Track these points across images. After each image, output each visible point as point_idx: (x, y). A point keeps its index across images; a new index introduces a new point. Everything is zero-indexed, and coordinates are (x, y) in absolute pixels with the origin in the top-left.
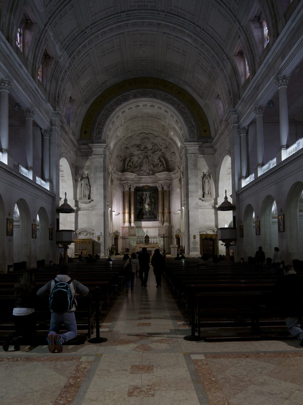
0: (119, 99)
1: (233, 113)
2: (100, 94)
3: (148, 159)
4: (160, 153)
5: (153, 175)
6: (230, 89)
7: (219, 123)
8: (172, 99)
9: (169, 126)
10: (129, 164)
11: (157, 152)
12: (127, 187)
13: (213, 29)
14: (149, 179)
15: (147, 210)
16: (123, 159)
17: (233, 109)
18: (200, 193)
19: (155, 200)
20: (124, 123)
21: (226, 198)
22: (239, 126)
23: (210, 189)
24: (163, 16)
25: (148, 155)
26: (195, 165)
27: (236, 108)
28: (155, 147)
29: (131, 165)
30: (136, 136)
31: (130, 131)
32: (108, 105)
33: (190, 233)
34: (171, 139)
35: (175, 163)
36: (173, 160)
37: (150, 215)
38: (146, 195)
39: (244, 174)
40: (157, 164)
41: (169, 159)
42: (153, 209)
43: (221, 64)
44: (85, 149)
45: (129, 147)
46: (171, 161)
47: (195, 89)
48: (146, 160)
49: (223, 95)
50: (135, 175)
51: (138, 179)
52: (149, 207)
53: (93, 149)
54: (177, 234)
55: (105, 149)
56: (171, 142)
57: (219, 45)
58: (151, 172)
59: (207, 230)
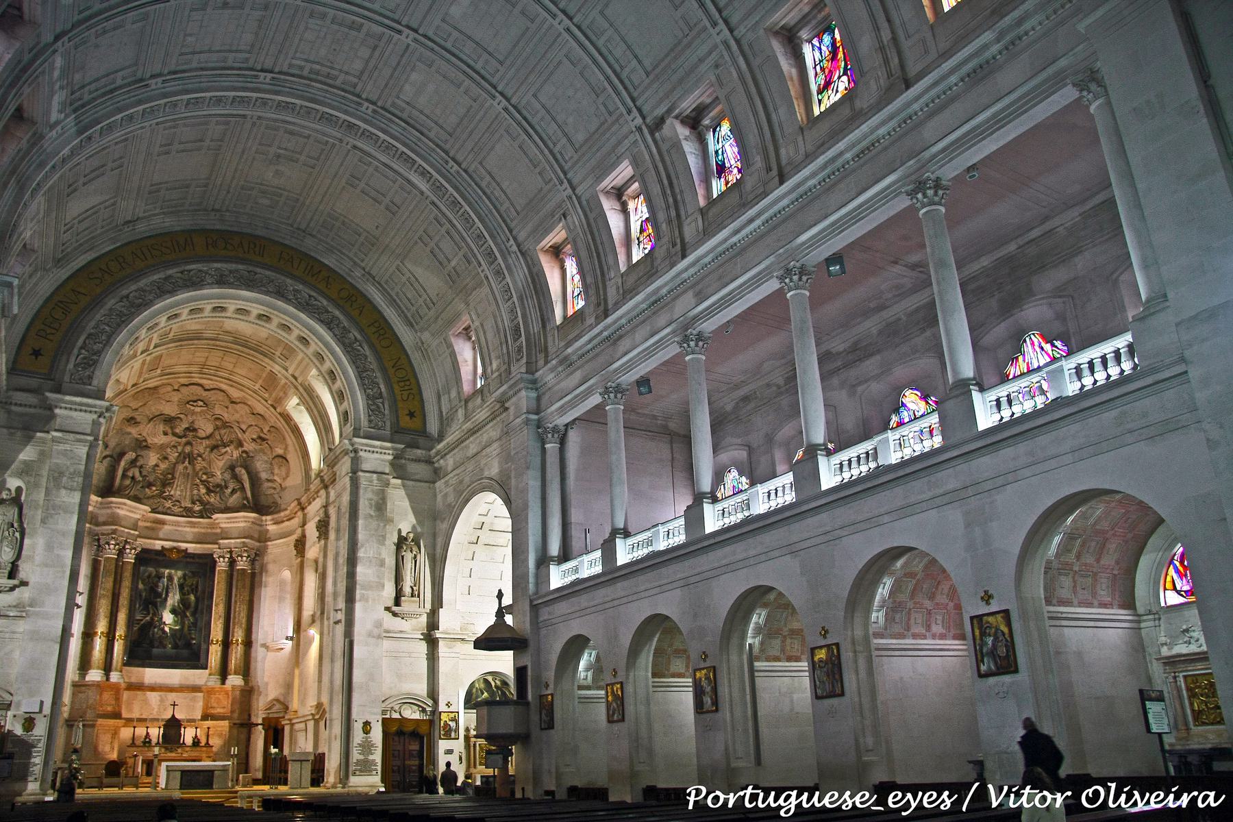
0: (170, 276)
1: (530, 386)
2: (107, 249)
3: (194, 465)
4: (236, 454)
5: (203, 517)
6: (519, 323)
7: (460, 401)
8: (327, 312)
9: (294, 381)
10: (130, 474)
11: (228, 449)
12: (112, 546)
13: (493, 178)
14: (188, 529)
15: (167, 629)
16: (107, 453)
17: (530, 377)
18: (389, 591)
20: (155, 347)
21: (500, 613)
22: (539, 420)
23: (416, 582)
24: (369, 112)
25: (196, 452)
26: (380, 506)
27: (538, 374)
28: (223, 432)
29: (137, 474)
30: (169, 388)
31: (159, 371)
32: (133, 287)
33: (354, 716)
34: (287, 418)
35: (283, 489)
36: (276, 478)
37: (175, 646)
38: (170, 578)
39: (554, 549)
40: (218, 486)
41: (264, 476)
42: (189, 627)
43: (500, 260)
44: (26, 405)
45: (139, 419)
46: (268, 481)
47: (395, 301)
48: (186, 468)
49: (485, 333)
50: (145, 511)
51: (148, 524)
52: (175, 621)
53: (57, 411)
54: (271, 716)
55: (100, 416)
56: (281, 424)
57: (501, 216)
58: (197, 508)
59: (405, 706)
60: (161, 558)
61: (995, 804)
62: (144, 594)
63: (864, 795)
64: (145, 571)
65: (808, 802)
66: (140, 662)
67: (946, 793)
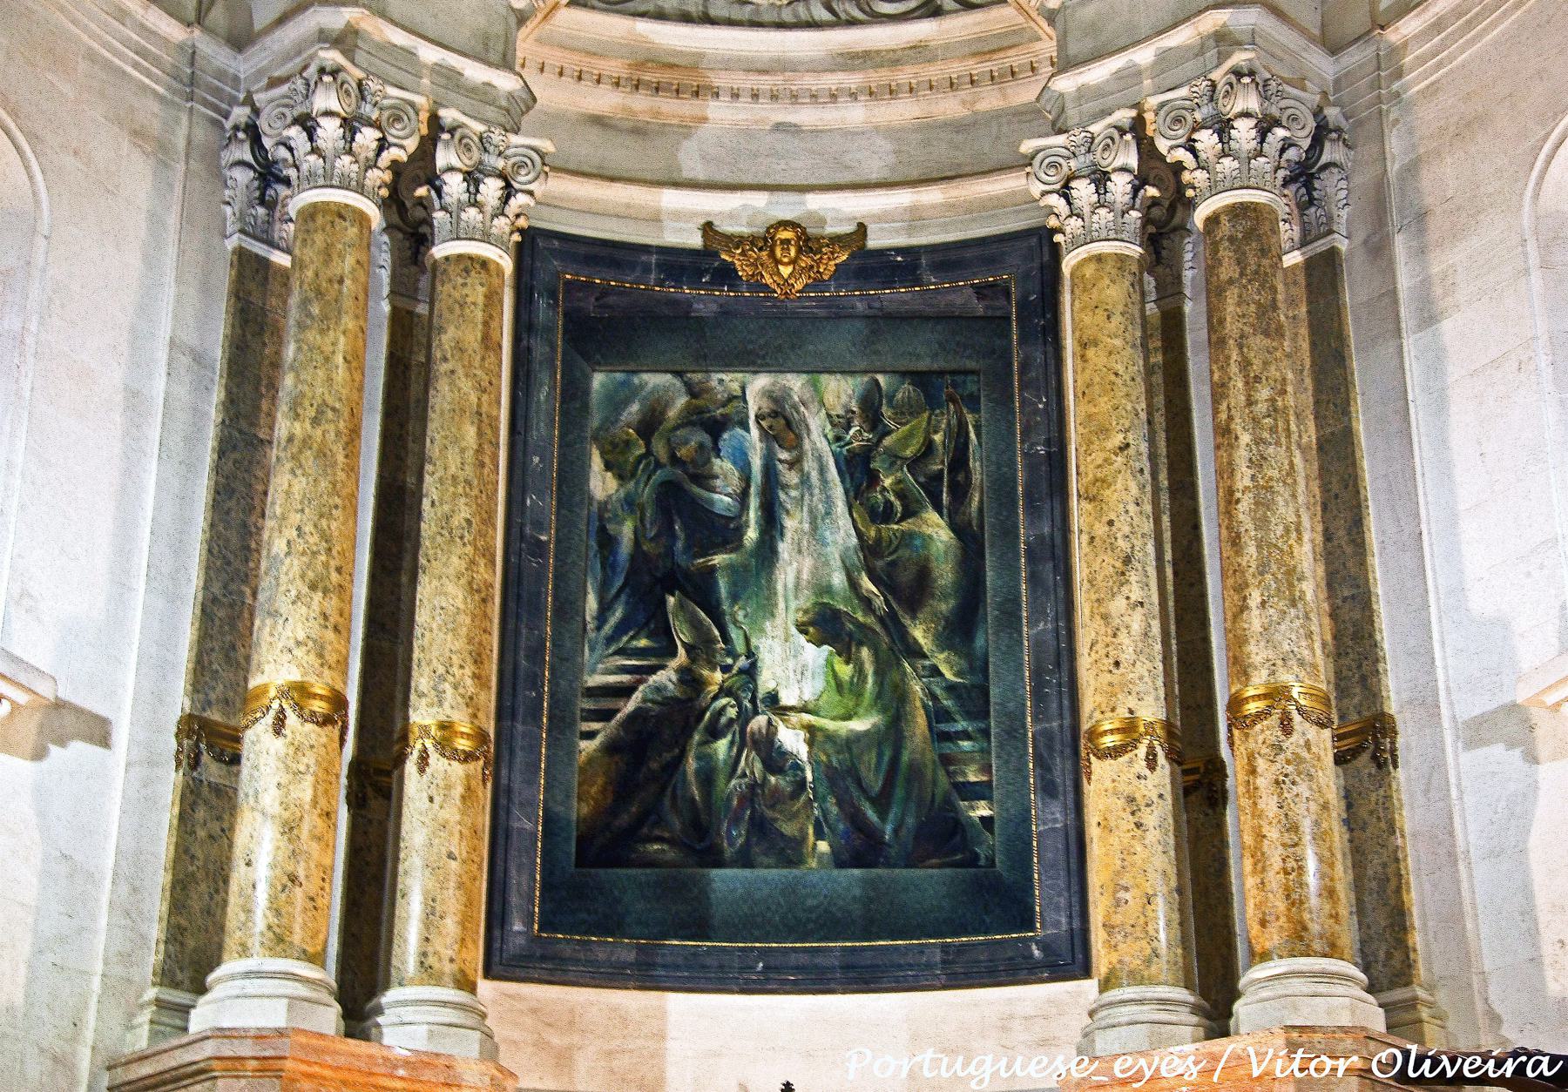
12: (330, 131)
14: (855, 114)
15: (791, 739)
19: (968, 538)
42: (938, 715)
51: (605, 101)
60: (703, 299)
62: (627, 531)
64: (616, 401)
66: (625, 950)
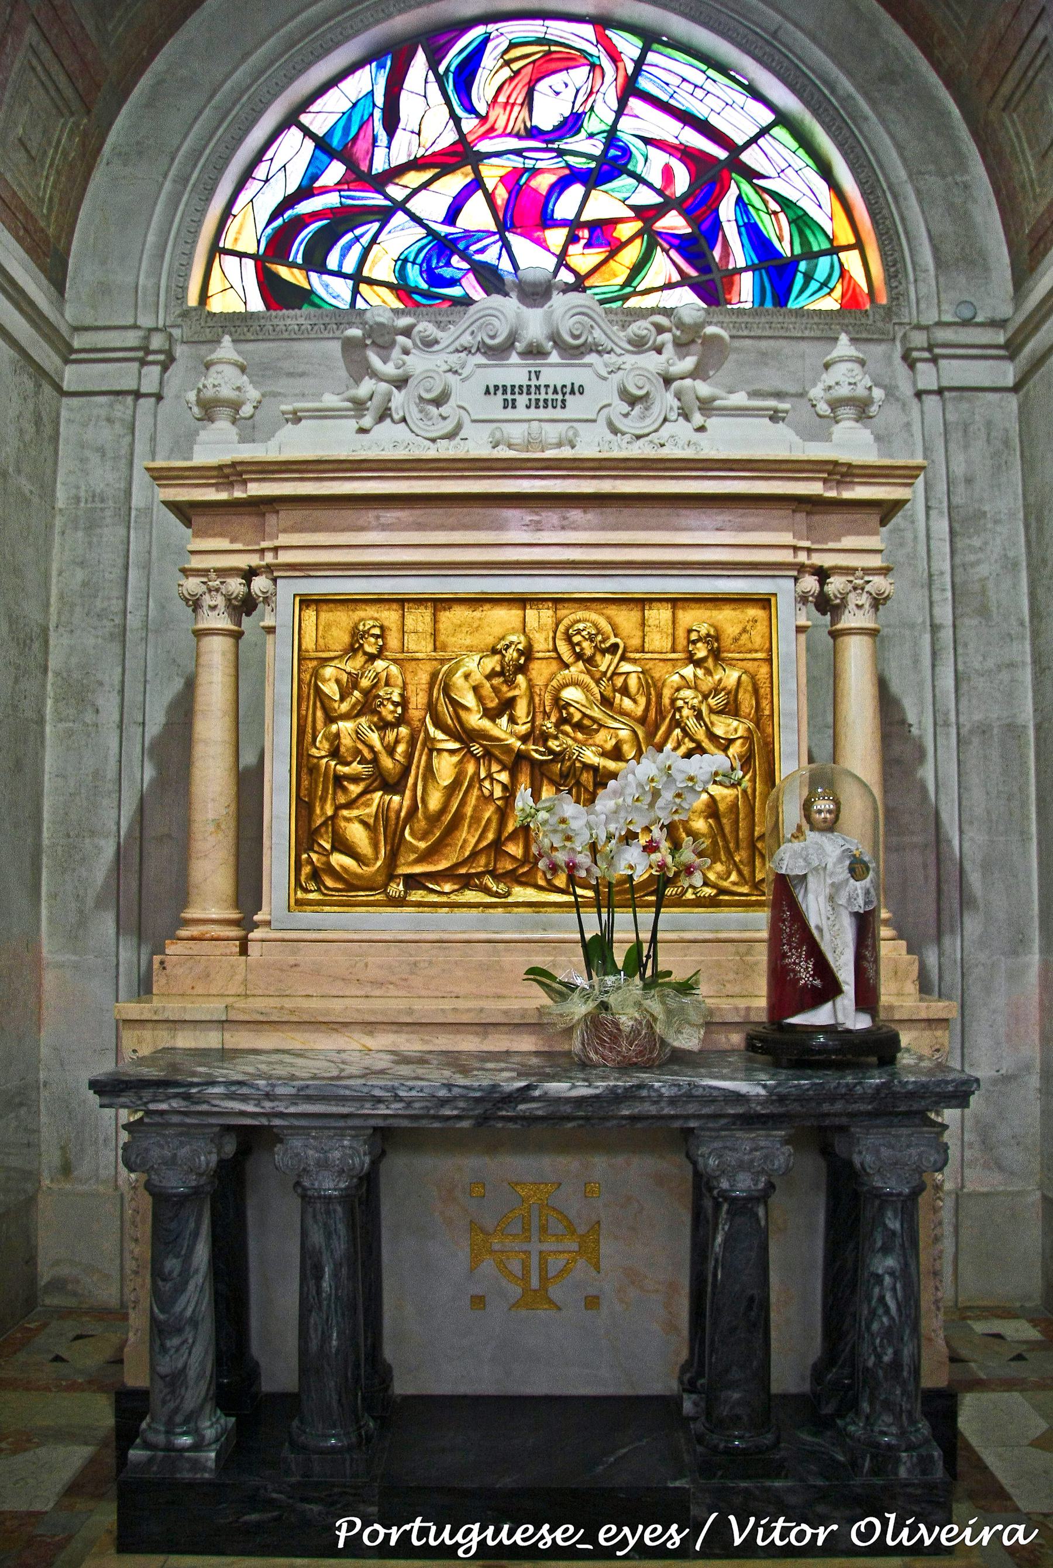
61: (738, 1541)
63: (566, 1530)
65: (494, 1539)
67: (675, 1527)
